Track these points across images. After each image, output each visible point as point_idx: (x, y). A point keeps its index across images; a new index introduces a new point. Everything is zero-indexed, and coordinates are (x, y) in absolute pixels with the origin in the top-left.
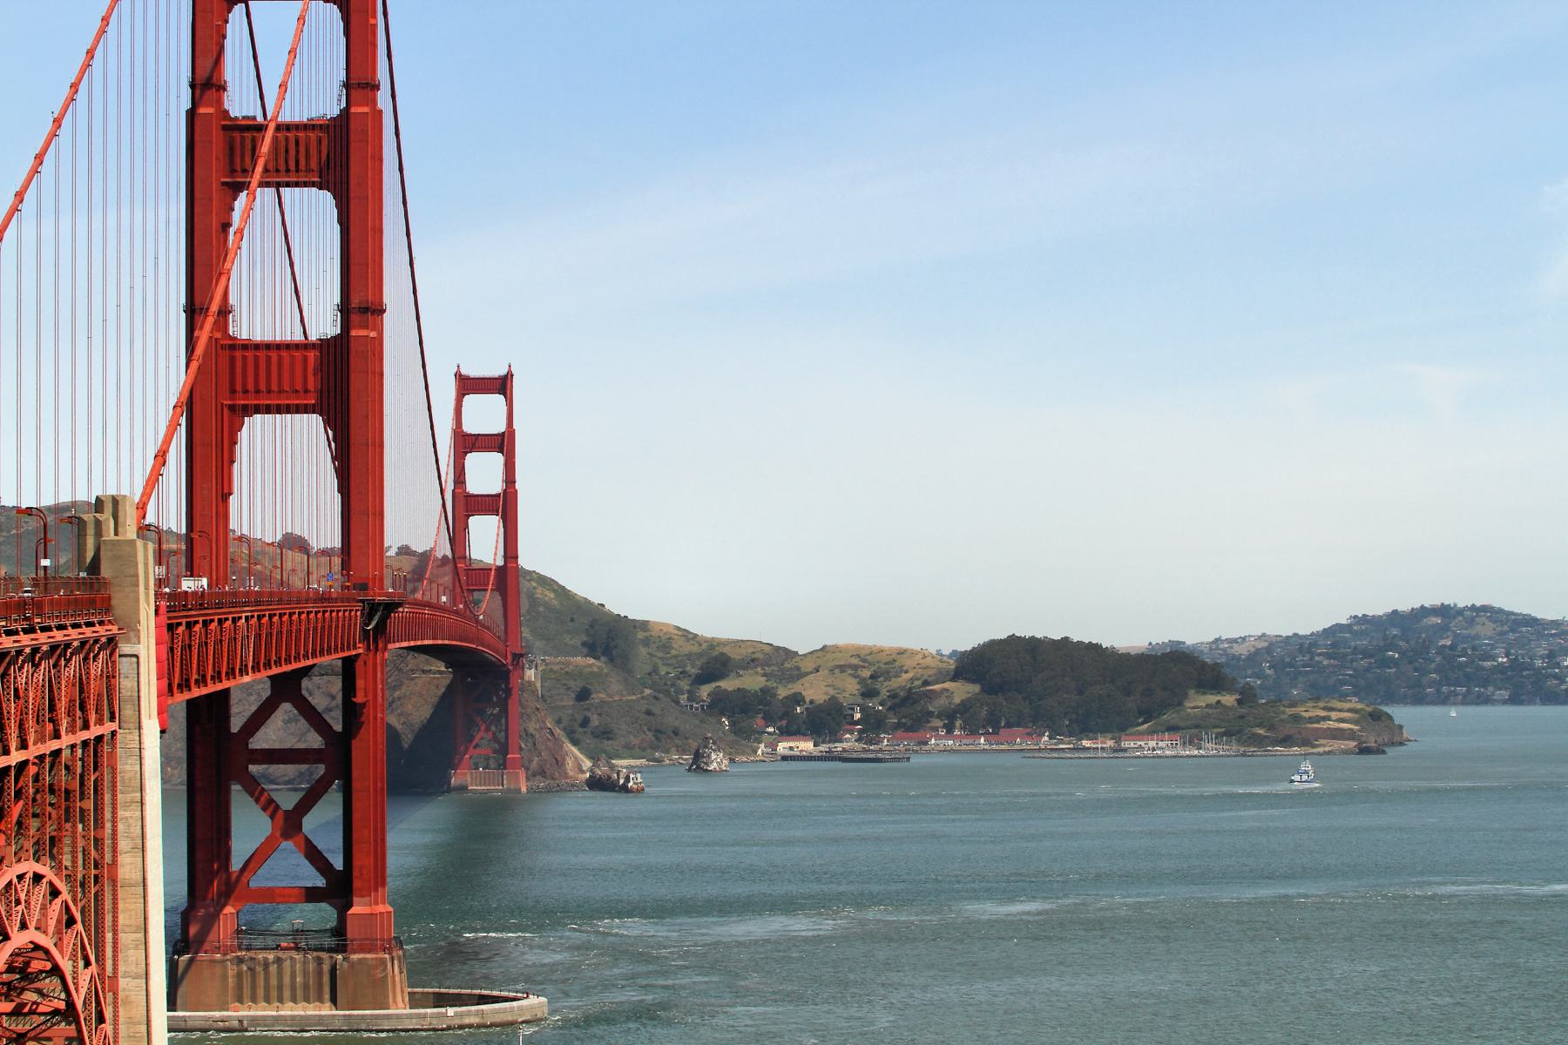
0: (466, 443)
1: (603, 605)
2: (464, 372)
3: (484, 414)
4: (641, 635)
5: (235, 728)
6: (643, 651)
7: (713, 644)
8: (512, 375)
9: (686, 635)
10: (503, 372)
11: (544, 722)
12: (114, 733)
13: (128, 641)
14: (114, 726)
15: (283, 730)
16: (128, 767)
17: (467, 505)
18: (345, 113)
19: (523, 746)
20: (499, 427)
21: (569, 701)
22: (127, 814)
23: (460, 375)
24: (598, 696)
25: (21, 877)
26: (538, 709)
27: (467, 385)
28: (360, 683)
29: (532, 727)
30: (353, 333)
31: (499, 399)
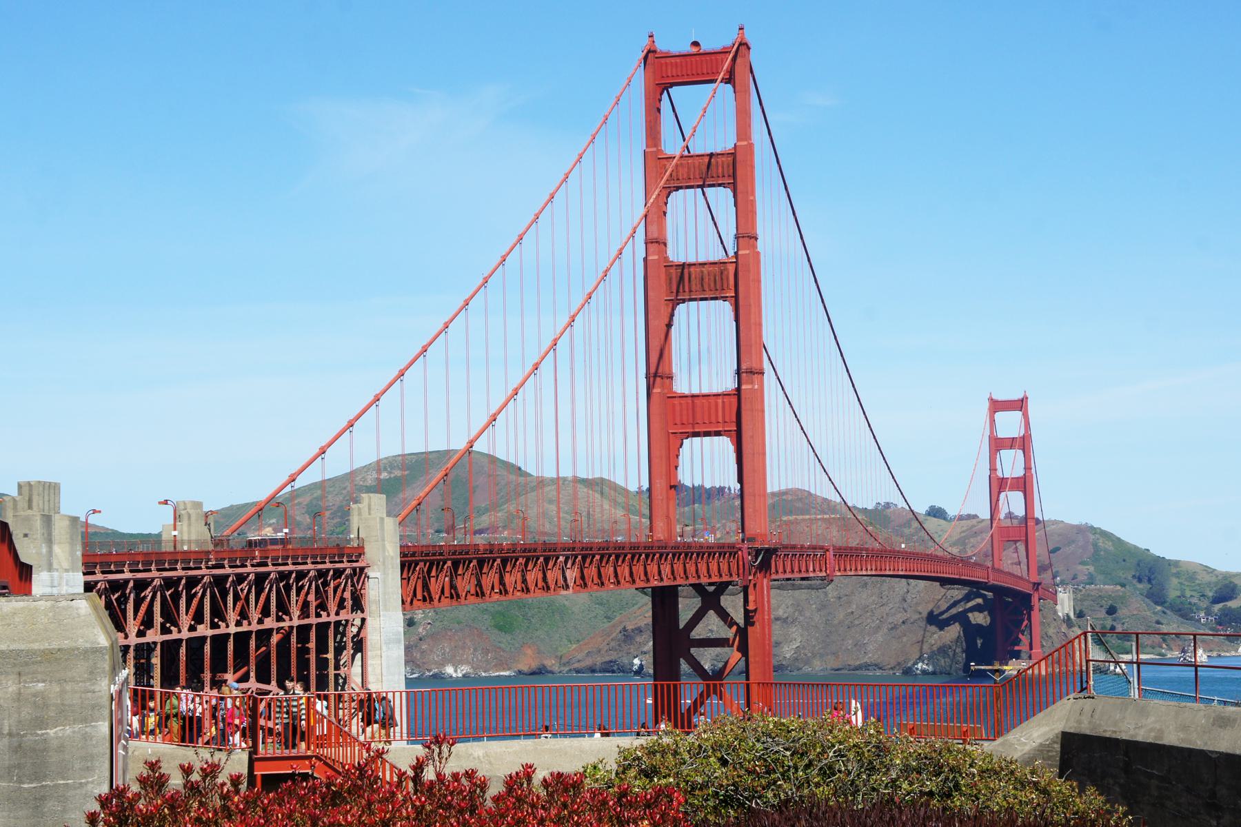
0: (997, 445)
1: (1148, 550)
2: (995, 397)
3: (1009, 424)
4: (1174, 570)
5: (681, 626)
6: (1175, 581)
7: (1227, 576)
8: (1027, 398)
9: (1209, 571)
10: (1021, 396)
11: (1060, 628)
13: (374, 571)
16: (374, 637)
17: (999, 485)
19: (1044, 644)
21: (1102, 614)
22: (374, 662)
23: (992, 399)
24: (1123, 612)
26: (1055, 620)
27: (997, 406)
28: (751, 598)
29: (1051, 631)
30: (744, 387)
31: (1019, 414)
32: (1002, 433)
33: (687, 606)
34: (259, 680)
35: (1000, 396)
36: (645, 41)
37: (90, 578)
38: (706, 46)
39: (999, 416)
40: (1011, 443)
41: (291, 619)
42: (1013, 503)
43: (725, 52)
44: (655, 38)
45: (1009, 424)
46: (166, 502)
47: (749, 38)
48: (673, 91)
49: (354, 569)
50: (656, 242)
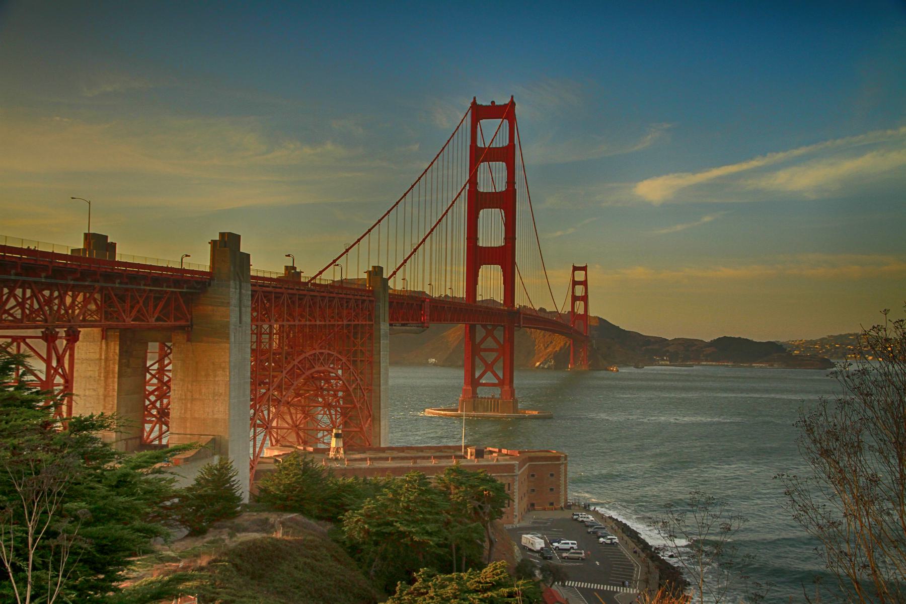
0: (575, 283)
12: (372, 324)
14: (371, 323)
15: (490, 343)
17: (575, 298)
18: (507, 190)
20: (582, 279)
25: (321, 354)
27: (575, 269)
31: (584, 272)
32: (576, 279)
33: (480, 333)
34: (329, 349)
35: (577, 265)
36: (472, 100)
37: (255, 288)
38: (497, 103)
39: (576, 272)
40: (580, 283)
41: (343, 321)
42: (580, 308)
43: (506, 105)
44: (476, 99)
45: (580, 276)
46: (289, 256)
47: (515, 100)
48: (481, 121)
49: (370, 301)
50: (473, 181)
